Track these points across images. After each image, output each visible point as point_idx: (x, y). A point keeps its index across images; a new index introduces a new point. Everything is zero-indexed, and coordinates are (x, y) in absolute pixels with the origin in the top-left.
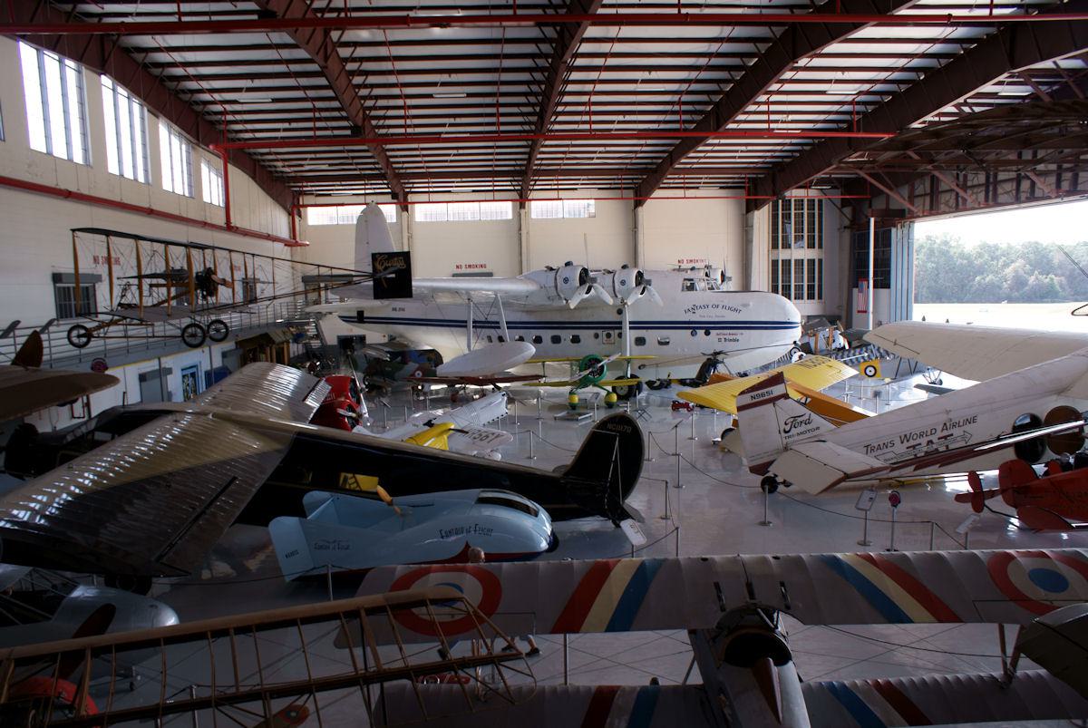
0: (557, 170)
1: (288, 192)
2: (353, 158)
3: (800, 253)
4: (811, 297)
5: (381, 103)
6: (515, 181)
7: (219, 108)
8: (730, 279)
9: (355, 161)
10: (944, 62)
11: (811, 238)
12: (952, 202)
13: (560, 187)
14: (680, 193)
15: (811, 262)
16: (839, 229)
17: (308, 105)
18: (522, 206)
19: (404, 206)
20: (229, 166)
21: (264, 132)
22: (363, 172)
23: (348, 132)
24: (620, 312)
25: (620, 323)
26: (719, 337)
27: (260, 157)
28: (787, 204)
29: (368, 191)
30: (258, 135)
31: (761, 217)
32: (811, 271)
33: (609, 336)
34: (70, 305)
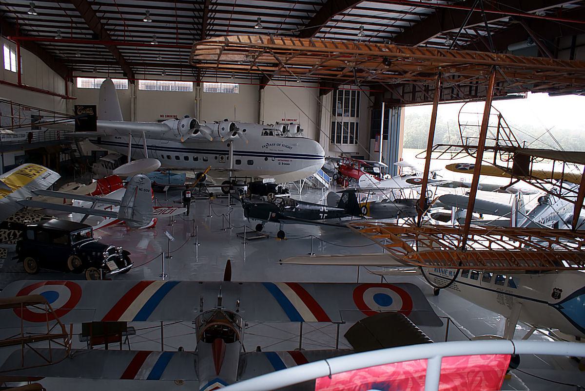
2: (100, 52)
3: (347, 119)
4: (351, 142)
5: (110, 22)
6: (194, 71)
8: (302, 130)
10: (412, 24)
11: (353, 112)
12: (423, 98)
14: (283, 83)
15: (352, 124)
16: (368, 108)
18: (198, 85)
19: (133, 81)
20: (11, 52)
24: (229, 145)
25: (228, 151)
26: (279, 162)
28: (341, 93)
29: (110, 71)
30: (41, 34)
31: (327, 99)
32: (352, 129)
33: (222, 158)
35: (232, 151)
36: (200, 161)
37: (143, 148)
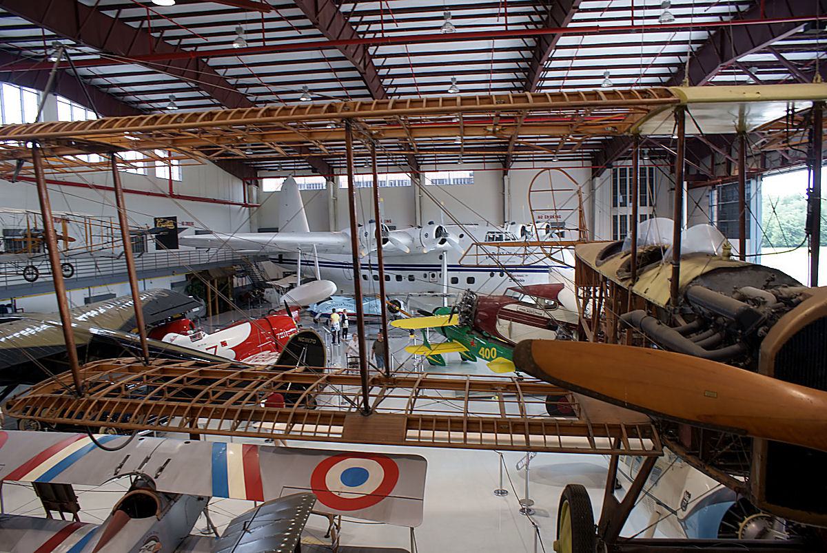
0: (483, 147)
13: (486, 160)
24: (441, 257)
25: (440, 266)
31: (605, 182)
35: (446, 266)
36: (405, 280)
37: (313, 265)
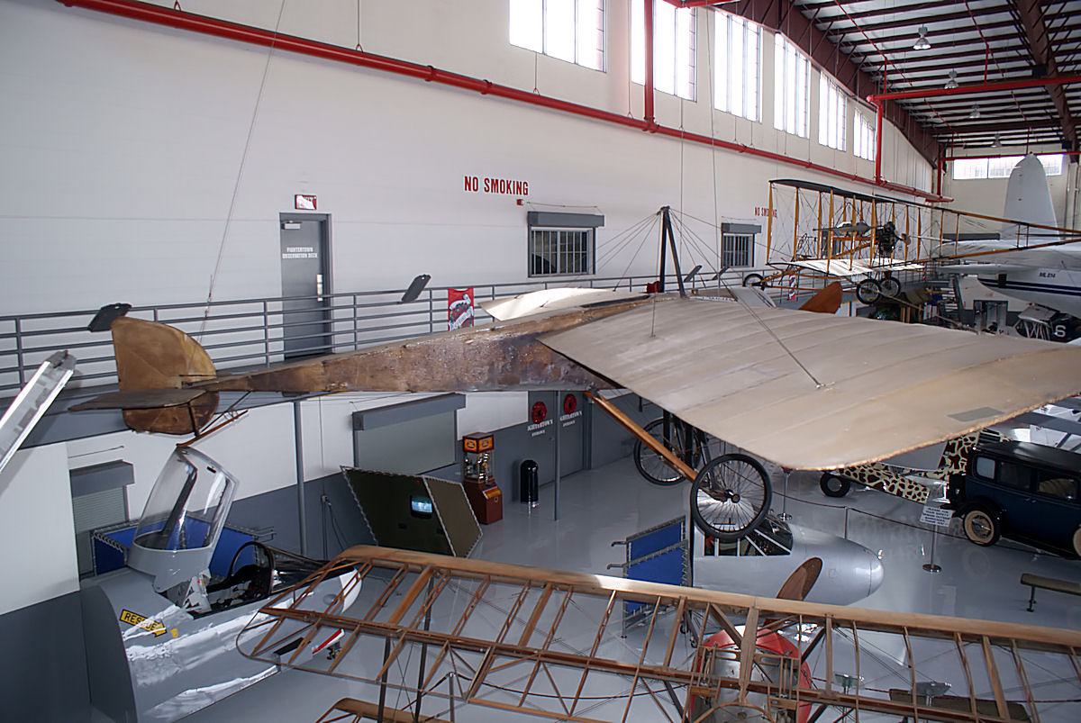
1: (935, 143)
2: (1021, 103)
7: (880, 58)
9: (1022, 106)
17: (982, 46)
21: (922, 80)
22: (1028, 119)
23: (1029, 73)
27: (911, 108)
29: (1030, 141)
30: (915, 84)
34: (732, 254)
